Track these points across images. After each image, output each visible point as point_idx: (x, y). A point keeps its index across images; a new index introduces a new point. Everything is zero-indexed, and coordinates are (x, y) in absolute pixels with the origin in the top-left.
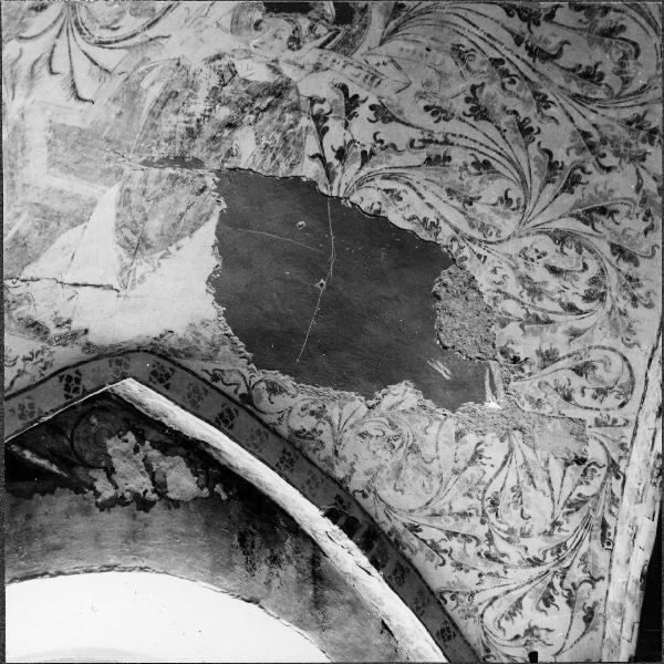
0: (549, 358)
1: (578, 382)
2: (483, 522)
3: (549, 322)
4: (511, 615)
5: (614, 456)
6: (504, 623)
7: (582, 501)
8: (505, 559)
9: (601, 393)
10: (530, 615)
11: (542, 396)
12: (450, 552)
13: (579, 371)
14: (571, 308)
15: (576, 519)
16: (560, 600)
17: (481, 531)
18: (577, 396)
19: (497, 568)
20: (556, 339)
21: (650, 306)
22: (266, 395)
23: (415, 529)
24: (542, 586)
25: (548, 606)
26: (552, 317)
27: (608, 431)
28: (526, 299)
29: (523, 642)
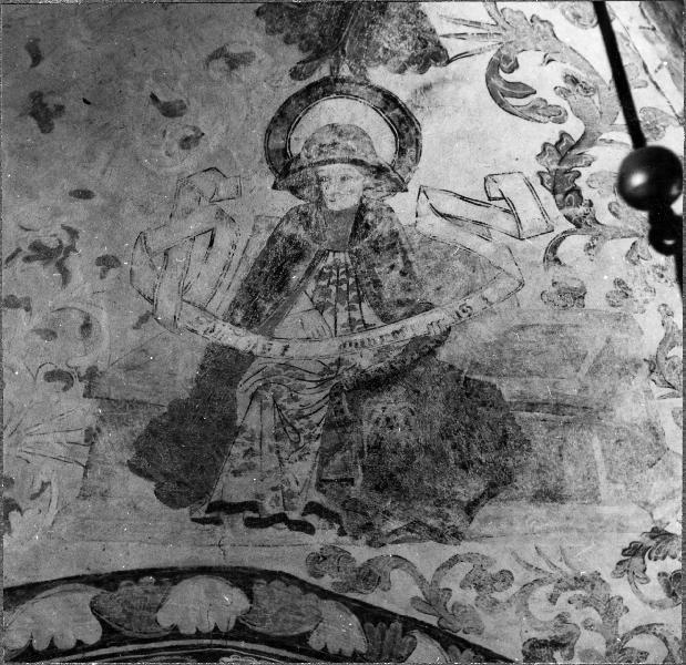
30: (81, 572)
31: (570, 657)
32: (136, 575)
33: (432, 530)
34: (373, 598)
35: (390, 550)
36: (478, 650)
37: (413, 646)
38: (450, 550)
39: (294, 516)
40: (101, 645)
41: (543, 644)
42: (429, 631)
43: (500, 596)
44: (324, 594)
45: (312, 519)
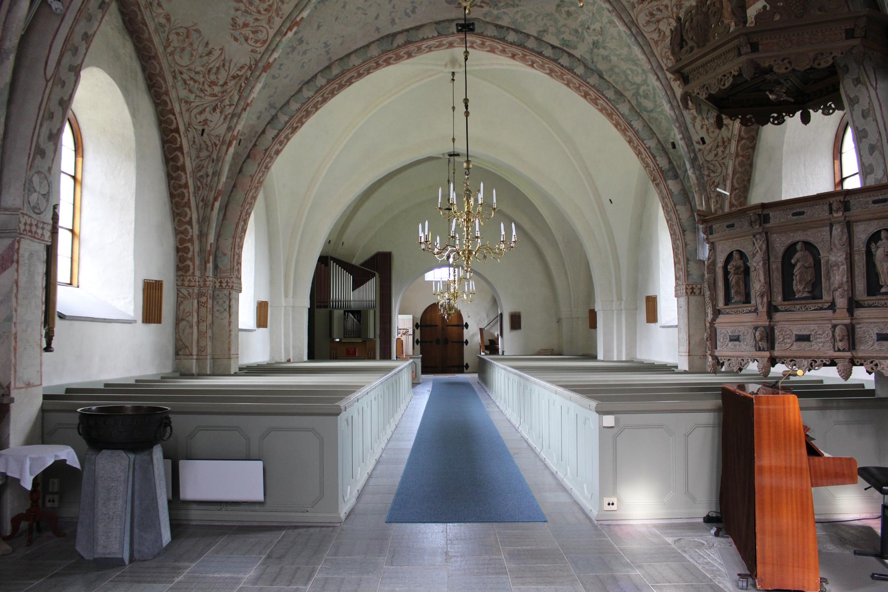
0: (246, 25)
1: (251, 36)
2: (203, 77)
3: (251, 14)
4: (201, 113)
5: (252, 63)
6: (198, 116)
7: (238, 76)
8: (205, 92)
9: (256, 41)
10: (207, 115)
11: (238, 38)
12: (189, 85)
13: (253, 32)
14: (259, 12)
15: (233, 82)
16: (218, 111)
17: (202, 80)
18: (249, 40)
19: (202, 95)
20: (250, 19)
21: (281, 18)
22: (156, 5)
23: (181, 73)
24: (214, 104)
25: (214, 112)
26: (252, 13)
27: (254, 55)
28: (247, 5)
29: (201, 124)
30: (430, 21)
31: (548, 34)
32: (444, 21)
33: (511, 5)
34: (500, 23)
35: (502, 10)
36: (524, 33)
37: (508, 34)
38: (516, 9)
39: (478, 4)
40: (438, 36)
41: (540, 32)
42: (513, 29)
43: (530, 20)
44: (488, 23)
45: (483, 4)
